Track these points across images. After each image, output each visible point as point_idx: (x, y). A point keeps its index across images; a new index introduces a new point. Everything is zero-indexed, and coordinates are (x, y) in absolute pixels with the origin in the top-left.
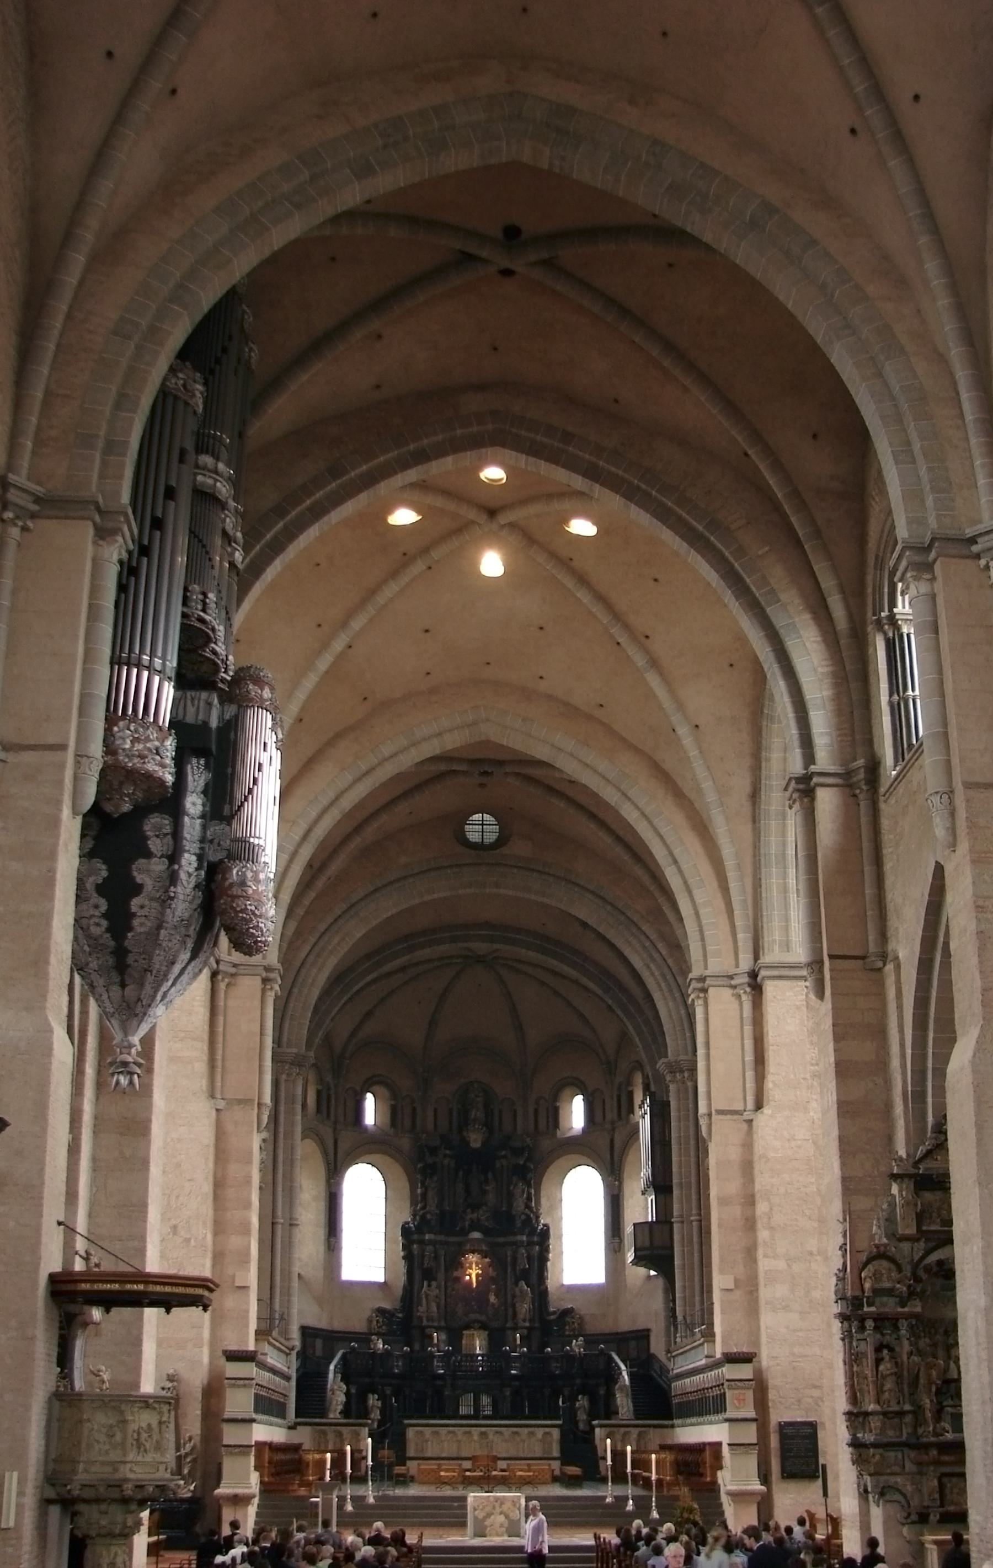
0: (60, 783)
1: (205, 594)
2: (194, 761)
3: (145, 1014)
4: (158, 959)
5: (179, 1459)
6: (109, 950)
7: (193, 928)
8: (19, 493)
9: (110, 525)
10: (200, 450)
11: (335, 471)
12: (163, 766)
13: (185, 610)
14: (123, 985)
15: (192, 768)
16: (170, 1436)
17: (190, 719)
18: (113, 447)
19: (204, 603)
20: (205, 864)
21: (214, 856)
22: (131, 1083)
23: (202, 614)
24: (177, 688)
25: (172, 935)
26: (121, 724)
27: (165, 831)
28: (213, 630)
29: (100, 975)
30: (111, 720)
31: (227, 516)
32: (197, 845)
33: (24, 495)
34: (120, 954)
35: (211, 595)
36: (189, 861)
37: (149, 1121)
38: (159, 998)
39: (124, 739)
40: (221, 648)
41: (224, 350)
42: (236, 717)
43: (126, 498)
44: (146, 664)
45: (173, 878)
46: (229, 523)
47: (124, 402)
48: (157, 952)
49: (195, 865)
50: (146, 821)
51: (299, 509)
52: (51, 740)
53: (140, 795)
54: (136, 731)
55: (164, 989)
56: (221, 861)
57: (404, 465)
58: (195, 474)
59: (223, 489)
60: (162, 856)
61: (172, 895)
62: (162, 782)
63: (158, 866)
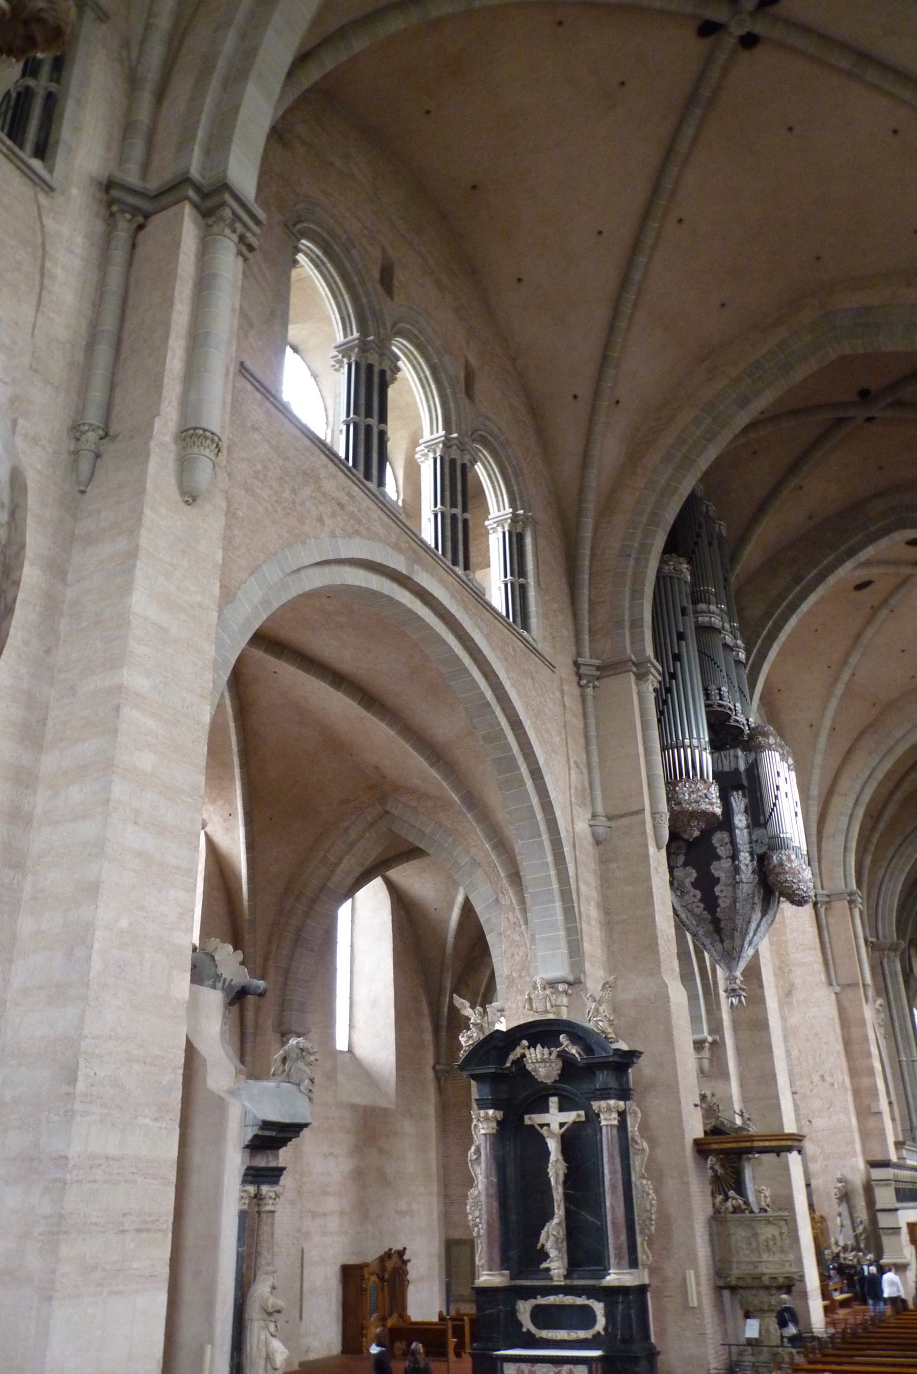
0: (644, 833)
1: (720, 690)
2: (735, 793)
3: (740, 957)
4: (739, 922)
5: (857, 1237)
6: (708, 921)
7: (756, 898)
8: (586, 667)
9: (643, 670)
10: (695, 602)
11: (797, 580)
12: (712, 804)
13: (709, 702)
14: (722, 941)
16: (847, 1222)
17: (726, 769)
18: (636, 624)
19: (720, 695)
20: (756, 857)
21: (760, 850)
22: (740, 1001)
23: (720, 702)
24: (712, 753)
26: (680, 784)
28: (730, 709)
30: (671, 784)
31: (725, 635)
32: (748, 846)
33: (591, 668)
34: (716, 922)
35: (723, 689)
36: (744, 857)
37: (767, 1019)
38: (746, 945)
39: (684, 794)
40: (741, 718)
41: (698, 536)
43: (650, 651)
44: (688, 744)
45: (737, 870)
46: (729, 639)
47: (637, 594)
48: (737, 917)
49: (749, 858)
51: (779, 611)
52: (635, 808)
53: (703, 825)
54: (690, 787)
55: (748, 939)
56: (765, 853)
57: (841, 561)
58: (697, 618)
59: (716, 622)
60: (727, 858)
61: (738, 880)
62: (714, 814)
63: (726, 864)
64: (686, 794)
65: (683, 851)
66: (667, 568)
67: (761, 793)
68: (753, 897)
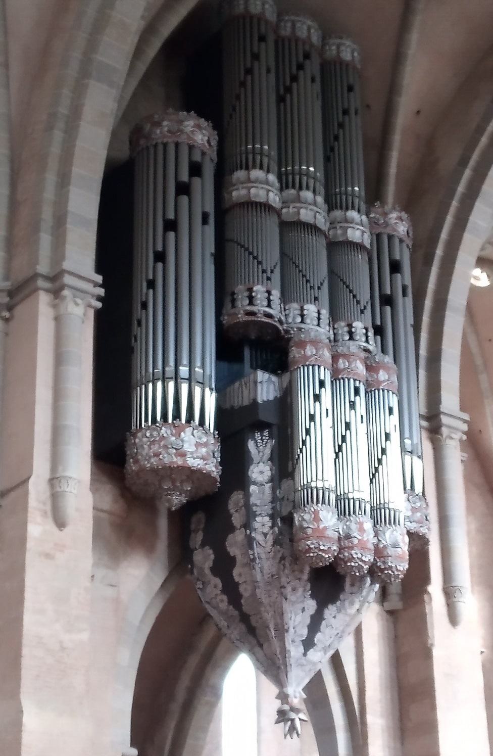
2: (258, 436)
4: (269, 617)
12: (183, 455)
15: (256, 442)
17: (246, 402)
21: (285, 513)
23: (248, 308)
25: (270, 591)
26: (139, 435)
27: (240, 505)
29: (244, 643)
32: (270, 506)
34: (245, 618)
36: (262, 523)
39: (142, 446)
42: (290, 382)
44: (173, 375)
45: (250, 542)
48: (263, 609)
49: (270, 524)
50: (230, 502)
60: (241, 527)
64: (145, 446)
65: (202, 526)
66: (158, 132)
67: (292, 428)
68: (279, 578)
